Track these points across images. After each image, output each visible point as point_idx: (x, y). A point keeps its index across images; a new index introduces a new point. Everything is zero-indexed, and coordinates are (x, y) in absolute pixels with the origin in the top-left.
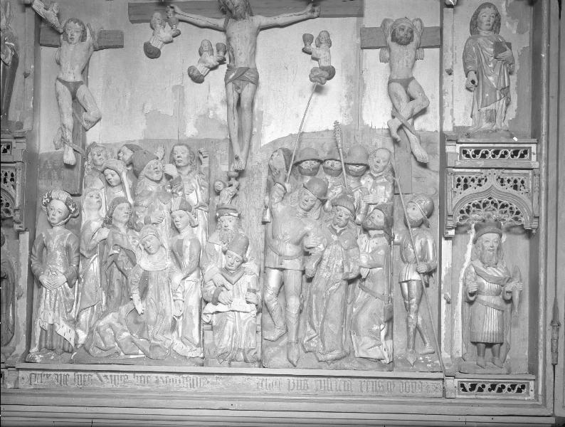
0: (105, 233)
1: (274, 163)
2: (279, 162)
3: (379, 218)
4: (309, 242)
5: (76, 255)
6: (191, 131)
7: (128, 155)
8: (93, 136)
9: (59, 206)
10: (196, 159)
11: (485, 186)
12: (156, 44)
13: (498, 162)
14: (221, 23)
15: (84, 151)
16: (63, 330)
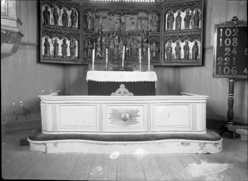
0: (105, 43)
1: (127, 34)
2: (127, 34)
3: (140, 41)
4: (132, 44)
5: (101, 46)
6: (116, 30)
7: (108, 33)
8: (103, 30)
9: (99, 40)
10: (117, 34)
11: (154, 38)
12: (111, 18)
13: (155, 35)
14: (120, 16)
15: (102, 33)
16: (100, 56)
